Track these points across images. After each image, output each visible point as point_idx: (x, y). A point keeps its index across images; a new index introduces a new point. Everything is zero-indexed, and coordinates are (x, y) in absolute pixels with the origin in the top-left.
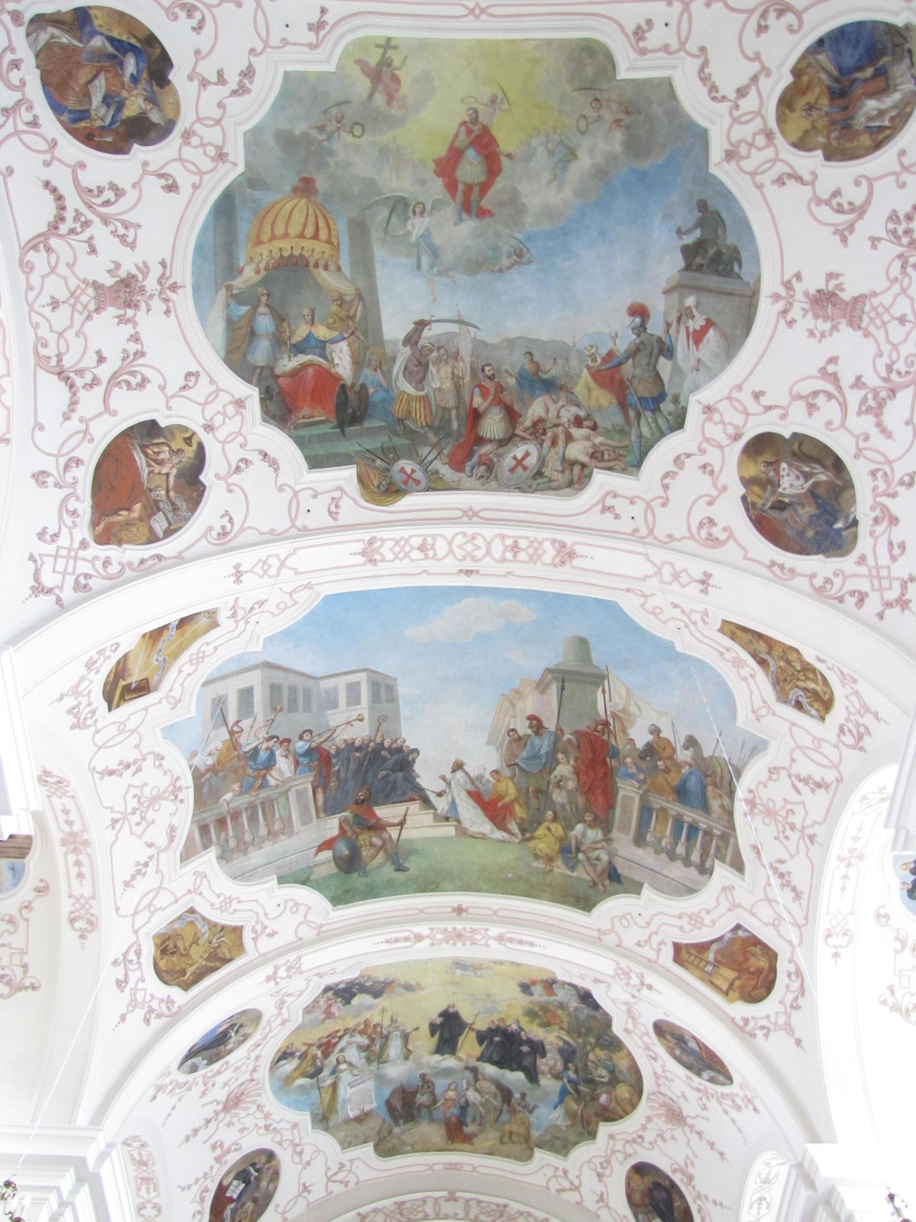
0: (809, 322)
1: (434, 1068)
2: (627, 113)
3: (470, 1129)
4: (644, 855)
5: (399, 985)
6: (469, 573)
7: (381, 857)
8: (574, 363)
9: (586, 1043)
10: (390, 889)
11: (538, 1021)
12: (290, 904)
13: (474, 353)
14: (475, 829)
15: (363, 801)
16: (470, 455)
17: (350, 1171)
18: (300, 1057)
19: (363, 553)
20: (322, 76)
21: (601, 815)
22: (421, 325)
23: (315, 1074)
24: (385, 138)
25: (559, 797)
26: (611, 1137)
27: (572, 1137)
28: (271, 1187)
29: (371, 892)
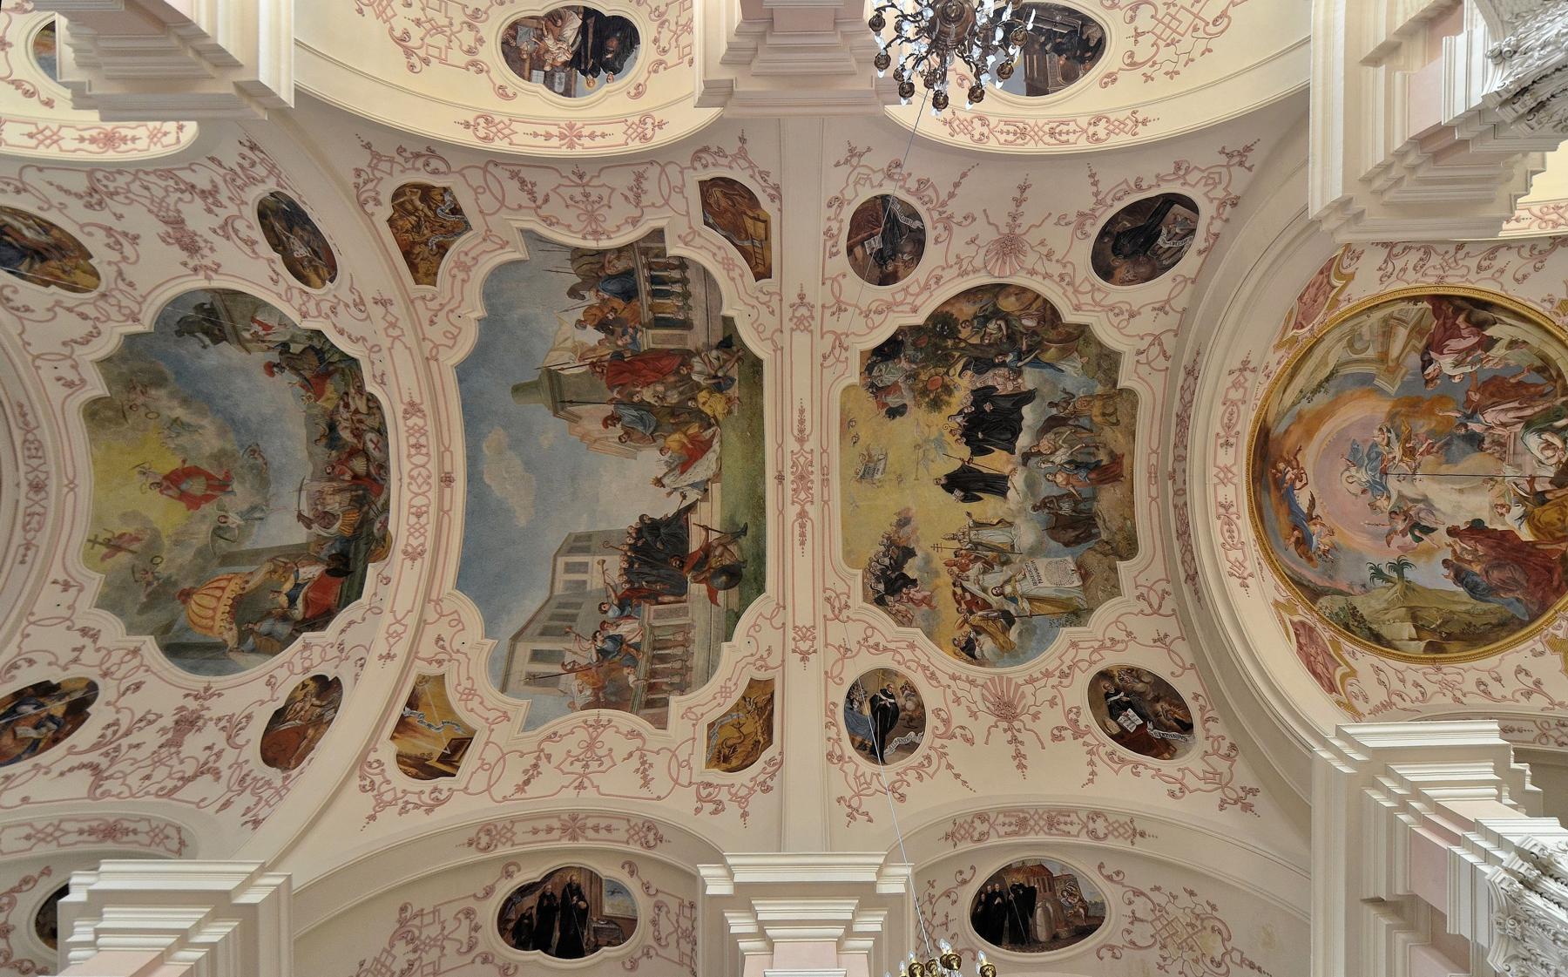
0: (206, 251)
1: (1025, 496)
2: (135, 388)
3: (1103, 457)
4: (698, 318)
5: (896, 532)
6: (447, 480)
7: (733, 548)
8: (315, 411)
9: (956, 348)
10: (760, 540)
11: (946, 398)
12: (752, 632)
13: (319, 479)
14: (714, 466)
15: (682, 562)
16: (375, 480)
17: (1150, 588)
18: (978, 633)
19: (413, 559)
20: (107, 584)
21: (678, 360)
22: (300, 517)
23: (1009, 619)
24: (166, 542)
25: (673, 398)
26: (1077, 308)
27: (1093, 350)
28: (1146, 679)
29: (760, 558)
